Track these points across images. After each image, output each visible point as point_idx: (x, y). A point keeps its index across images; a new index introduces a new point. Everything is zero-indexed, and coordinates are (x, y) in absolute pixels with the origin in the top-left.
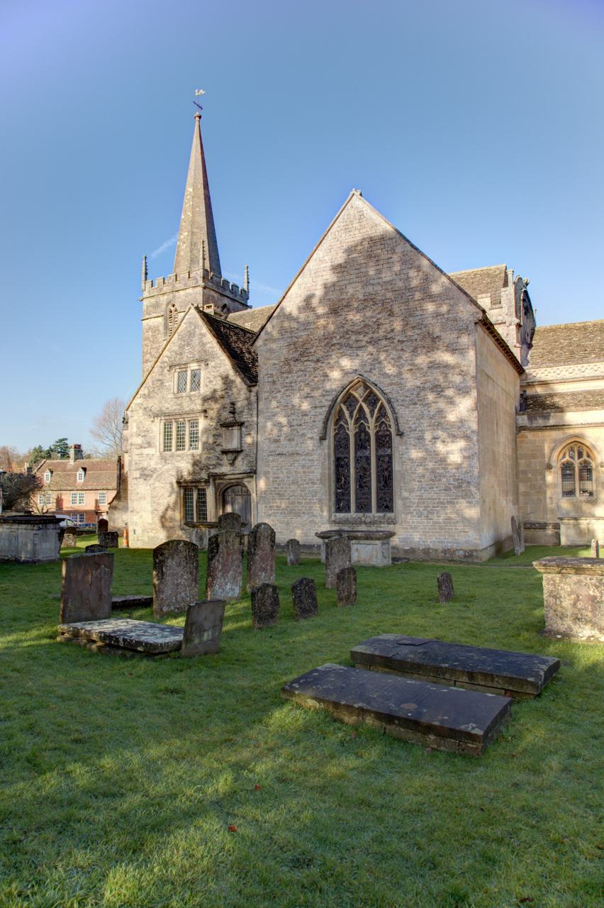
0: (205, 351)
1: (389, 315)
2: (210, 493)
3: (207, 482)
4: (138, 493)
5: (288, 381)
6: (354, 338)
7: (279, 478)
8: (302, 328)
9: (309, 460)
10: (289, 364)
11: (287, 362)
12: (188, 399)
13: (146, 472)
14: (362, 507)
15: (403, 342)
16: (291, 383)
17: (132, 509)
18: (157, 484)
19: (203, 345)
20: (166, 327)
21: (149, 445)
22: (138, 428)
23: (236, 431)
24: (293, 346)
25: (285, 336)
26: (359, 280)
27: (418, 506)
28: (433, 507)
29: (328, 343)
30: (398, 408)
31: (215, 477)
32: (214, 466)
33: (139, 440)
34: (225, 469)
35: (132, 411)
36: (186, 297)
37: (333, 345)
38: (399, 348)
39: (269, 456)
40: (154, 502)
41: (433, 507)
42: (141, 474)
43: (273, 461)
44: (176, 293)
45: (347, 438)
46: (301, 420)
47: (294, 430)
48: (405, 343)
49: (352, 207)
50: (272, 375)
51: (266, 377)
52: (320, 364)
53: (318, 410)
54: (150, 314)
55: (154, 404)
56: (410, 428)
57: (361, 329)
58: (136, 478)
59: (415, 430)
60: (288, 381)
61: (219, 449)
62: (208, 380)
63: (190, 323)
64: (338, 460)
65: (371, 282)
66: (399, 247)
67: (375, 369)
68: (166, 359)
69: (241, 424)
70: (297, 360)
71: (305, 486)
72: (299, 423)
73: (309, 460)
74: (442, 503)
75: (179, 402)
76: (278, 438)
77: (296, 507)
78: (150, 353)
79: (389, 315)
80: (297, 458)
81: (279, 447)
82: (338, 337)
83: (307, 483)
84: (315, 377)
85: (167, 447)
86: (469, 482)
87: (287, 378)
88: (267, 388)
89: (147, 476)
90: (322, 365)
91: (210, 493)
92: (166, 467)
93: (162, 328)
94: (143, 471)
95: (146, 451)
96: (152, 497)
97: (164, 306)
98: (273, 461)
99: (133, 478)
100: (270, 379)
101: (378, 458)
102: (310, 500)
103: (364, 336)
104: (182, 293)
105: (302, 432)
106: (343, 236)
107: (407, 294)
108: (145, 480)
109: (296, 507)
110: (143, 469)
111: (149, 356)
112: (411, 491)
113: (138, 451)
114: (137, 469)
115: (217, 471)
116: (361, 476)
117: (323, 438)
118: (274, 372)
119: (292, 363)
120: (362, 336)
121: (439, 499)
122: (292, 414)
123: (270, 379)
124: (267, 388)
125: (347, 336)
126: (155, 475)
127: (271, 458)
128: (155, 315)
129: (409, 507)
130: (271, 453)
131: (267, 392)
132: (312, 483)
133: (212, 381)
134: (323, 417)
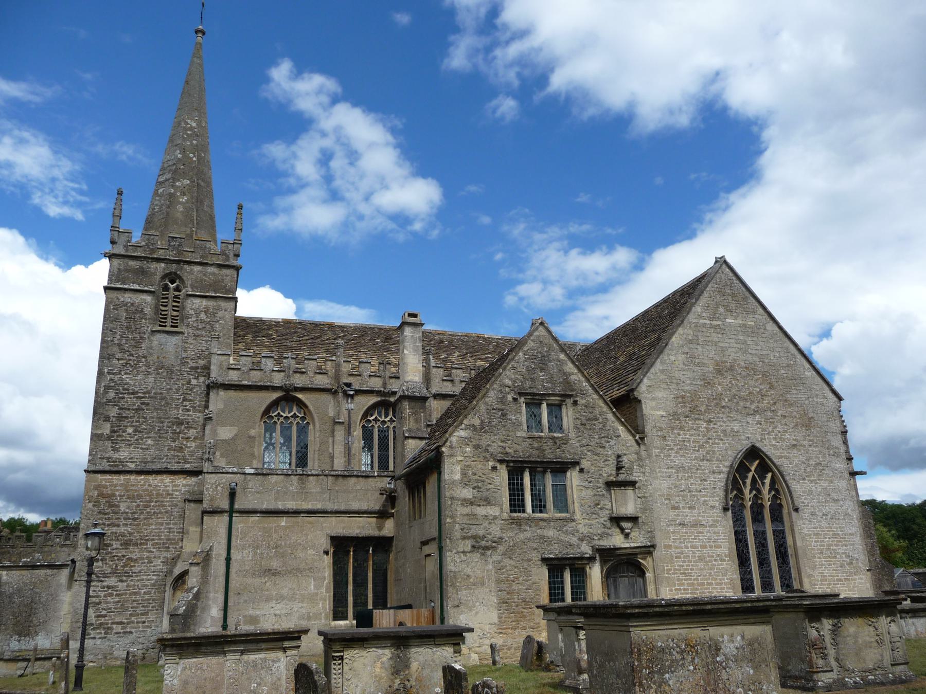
0: (568, 383)
1: (770, 388)
2: (595, 573)
3: (592, 559)
4: (468, 576)
5: (680, 438)
6: (741, 404)
7: (683, 553)
8: (688, 382)
9: (714, 533)
10: (679, 419)
11: (675, 415)
12: (550, 443)
13: (483, 543)
14: (766, 588)
15: (785, 417)
16: (684, 441)
17: (456, 603)
18: (507, 562)
19: (567, 375)
20: (157, 310)
21: (488, 502)
22: (464, 474)
23: (630, 492)
24: (680, 400)
25: (671, 387)
26: (738, 346)
27: (821, 584)
28: (834, 584)
29: (717, 404)
30: (790, 482)
31: (606, 555)
32: (602, 536)
33: (468, 493)
34: (617, 540)
35: (451, 447)
36: (204, 275)
37: (723, 407)
38: (783, 422)
39: (668, 526)
40: (500, 590)
41: (834, 584)
42: (473, 547)
43: (673, 532)
44: (186, 266)
45: (762, 506)
46: (700, 485)
47: (694, 495)
48: (787, 418)
49: (723, 272)
50: (661, 429)
51: (654, 430)
52: (712, 425)
53: (716, 476)
54: (123, 283)
55: (494, 443)
56: (803, 503)
57: (747, 395)
58: (463, 552)
59: (808, 506)
60: (680, 438)
61: (604, 516)
62: (579, 422)
63: (541, 342)
64: (736, 533)
65: (750, 351)
66: (769, 324)
67: (765, 439)
68: (508, 382)
69: (633, 484)
70: (687, 417)
71: (714, 563)
72: (699, 488)
73: (714, 533)
74: (840, 580)
75: (536, 445)
76: (676, 505)
77: (706, 589)
78: (119, 345)
79: (770, 388)
80: (701, 529)
81: (678, 515)
82: (726, 400)
83: (716, 560)
84: (709, 439)
85: (516, 504)
86: (857, 559)
87: (679, 435)
88: (658, 443)
89: (487, 548)
90: (715, 426)
91: (595, 573)
92: (521, 536)
93: (147, 310)
94: (477, 542)
95: (481, 511)
96: (499, 581)
97: (158, 277)
98: (673, 532)
99: (458, 552)
100: (659, 434)
101: (756, 533)
102: (720, 579)
103: (751, 404)
104: (197, 268)
105: (703, 499)
106: (718, 298)
107: (783, 372)
108: (483, 554)
109: (706, 589)
110: (475, 537)
111: (116, 349)
112: (814, 568)
113: (466, 510)
114: (464, 538)
115: (606, 543)
116: (759, 552)
117: (725, 509)
118: (664, 426)
119: (682, 418)
120: (749, 403)
121: (837, 576)
122: (689, 476)
123: (659, 434)
124: (658, 443)
125: (735, 401)
126: (501, 548)
127: (671, 529)
128: (136, 287)
129: (815, 585)
130: (672, 522)
131: (658, 448)
132: (721, 560)
133: (582, 424)
134: (723, 484)
